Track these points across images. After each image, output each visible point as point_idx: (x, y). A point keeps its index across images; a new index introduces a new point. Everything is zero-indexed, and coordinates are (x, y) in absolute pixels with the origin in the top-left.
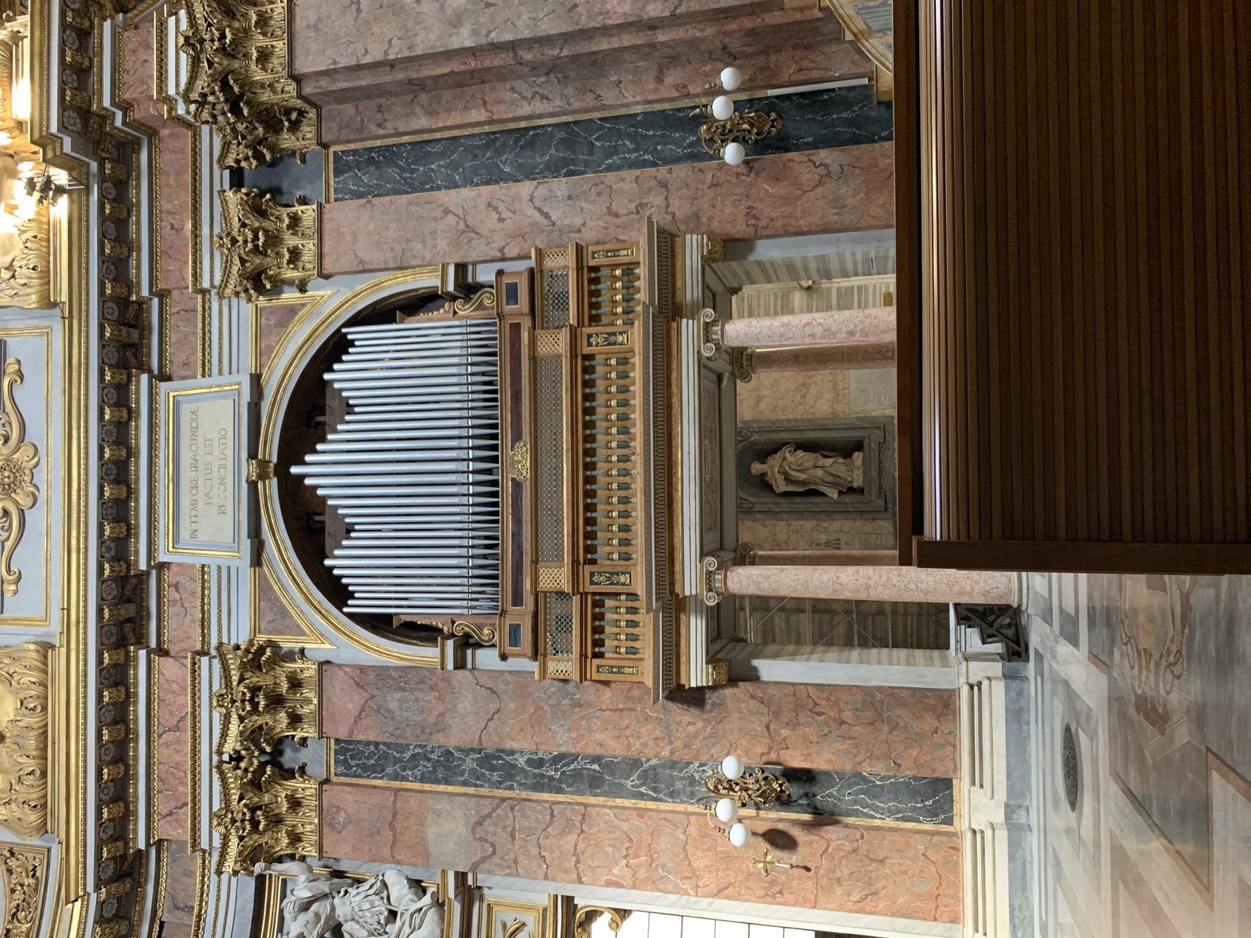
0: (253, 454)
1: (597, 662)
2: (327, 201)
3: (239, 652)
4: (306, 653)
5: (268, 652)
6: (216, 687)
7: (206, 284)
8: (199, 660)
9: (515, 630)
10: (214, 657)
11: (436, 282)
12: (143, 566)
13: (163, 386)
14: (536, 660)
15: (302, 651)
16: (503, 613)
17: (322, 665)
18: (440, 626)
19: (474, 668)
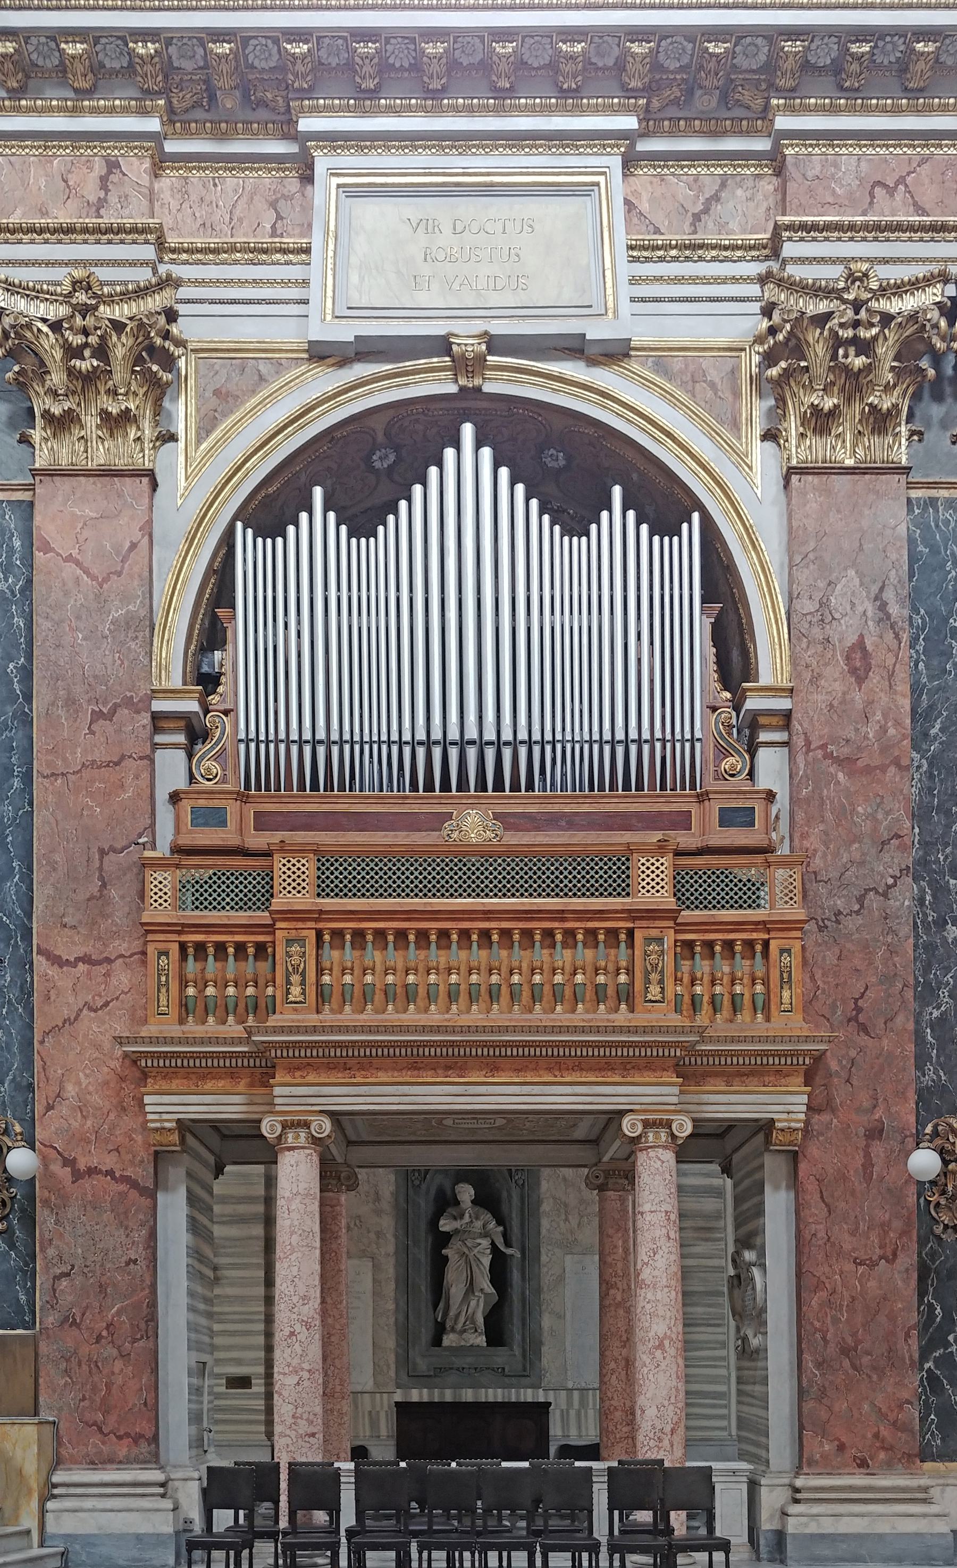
0: (495, 344)
1: (174, 949)
2: (910, 485)
3: (162, 320)
4: (170, 445)
5: (166, 377)
6: (103, 274)
7: (789, 249)
8: (147, 242)
9: (216, 818)
10: (155, 271)
11: (765, 678)
12: (306, 124)
13: (615, 163)
14: (173, 851)
15: (173, 438)
16: (243, 798)
17: (151, 475)
18: (220, 689)
19: (155, 746)
